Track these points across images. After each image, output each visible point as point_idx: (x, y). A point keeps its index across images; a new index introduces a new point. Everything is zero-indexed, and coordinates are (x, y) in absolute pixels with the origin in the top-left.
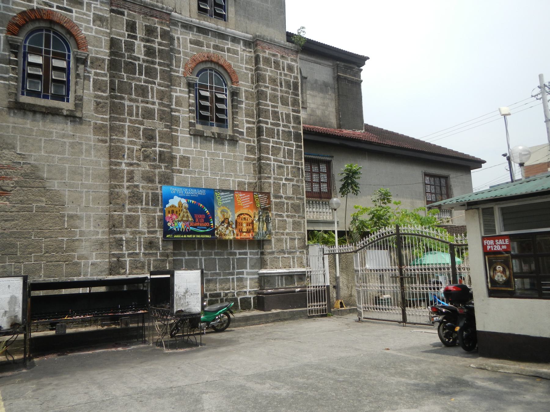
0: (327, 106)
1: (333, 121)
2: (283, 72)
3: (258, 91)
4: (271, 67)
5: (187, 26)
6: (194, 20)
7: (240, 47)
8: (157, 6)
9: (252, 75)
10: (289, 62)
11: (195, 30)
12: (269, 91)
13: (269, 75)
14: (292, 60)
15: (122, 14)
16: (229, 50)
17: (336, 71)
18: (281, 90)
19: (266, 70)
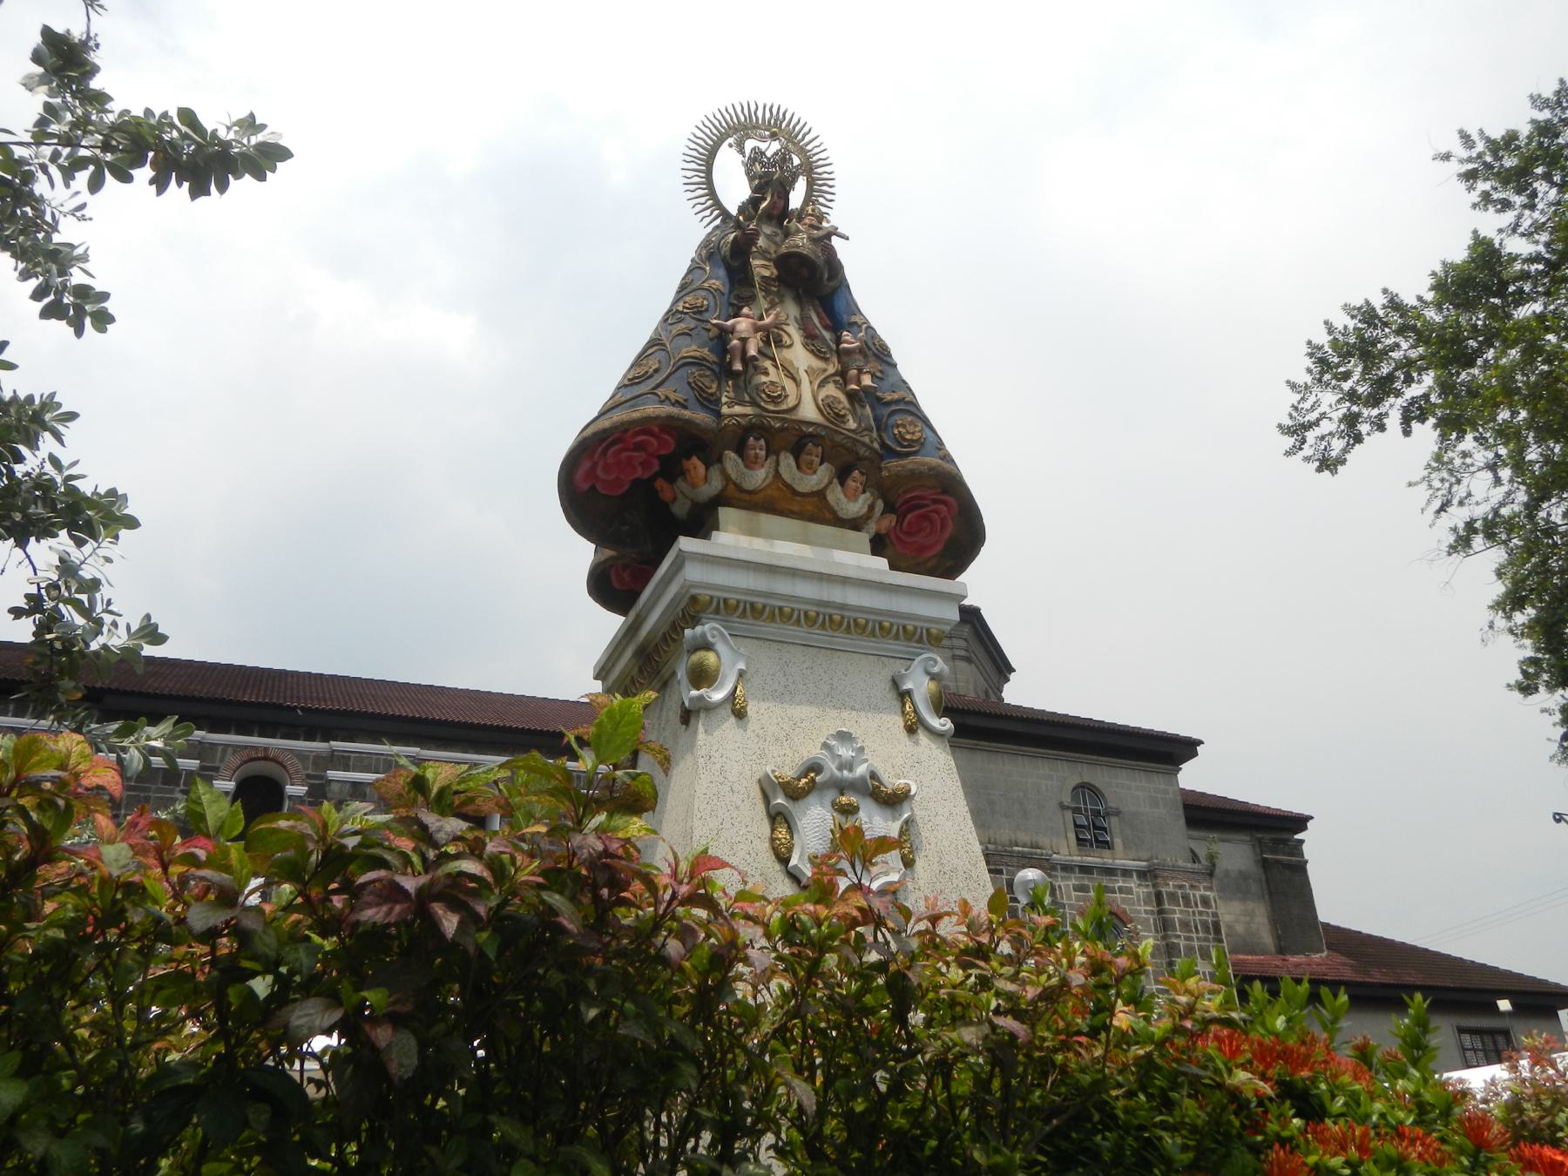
0: (1251, 914)
1: (1267, 939)
2: (1195, 909)
3: (1167, 945)
4: (1179, 906)
5: (1067, 868)
6: (1075, 858)
7: (1133, 883)
8: (1036, 854)
9: (1154, 920)
10: (1202, 892)
11: (1077, 869)
12: (1182, 943)
13: (1179, 919)
14: (1206, 889)
15: (1000, 872)
16: (1121, 890)
17: (1258, 850)
18: (1198, 938)
19: (1174, 912)
